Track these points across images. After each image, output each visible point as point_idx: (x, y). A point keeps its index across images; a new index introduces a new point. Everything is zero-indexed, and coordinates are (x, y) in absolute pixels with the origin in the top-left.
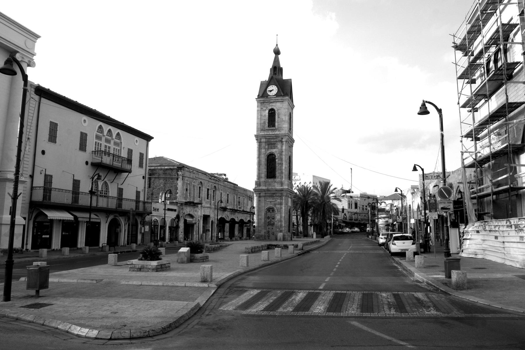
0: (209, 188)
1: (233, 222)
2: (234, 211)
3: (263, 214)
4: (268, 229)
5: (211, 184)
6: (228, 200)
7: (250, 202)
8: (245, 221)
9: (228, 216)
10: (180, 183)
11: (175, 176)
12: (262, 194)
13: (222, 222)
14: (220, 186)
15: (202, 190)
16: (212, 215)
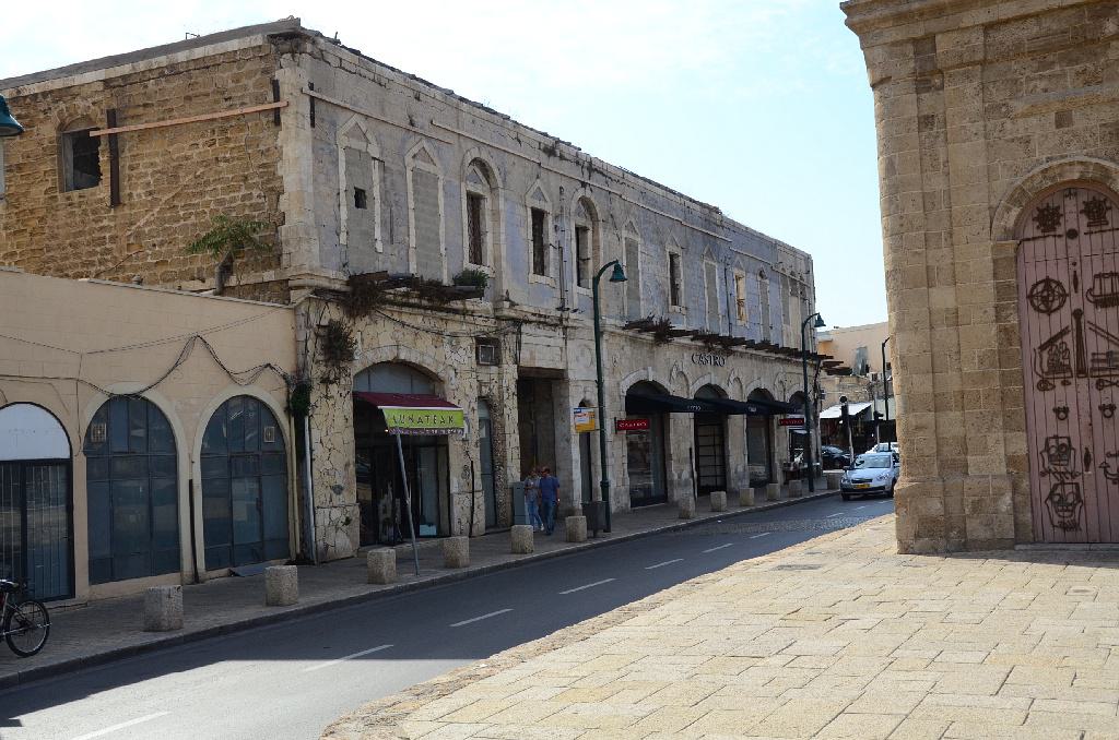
0: (547, 207)
1: (712, 409)
2: (717, 345)
3: (979, 258)
4: (1047, 426)
5: (555, 182)
6: (675, 287)
7: (794, 302)
8: (778, 396)
9: (680, 372)
10: (295, 150)
11: (259, 100)
12: (943, 44)
13: (648, 404)
14: (617, 204)
15: (496, 214)
16: (580, 372)
